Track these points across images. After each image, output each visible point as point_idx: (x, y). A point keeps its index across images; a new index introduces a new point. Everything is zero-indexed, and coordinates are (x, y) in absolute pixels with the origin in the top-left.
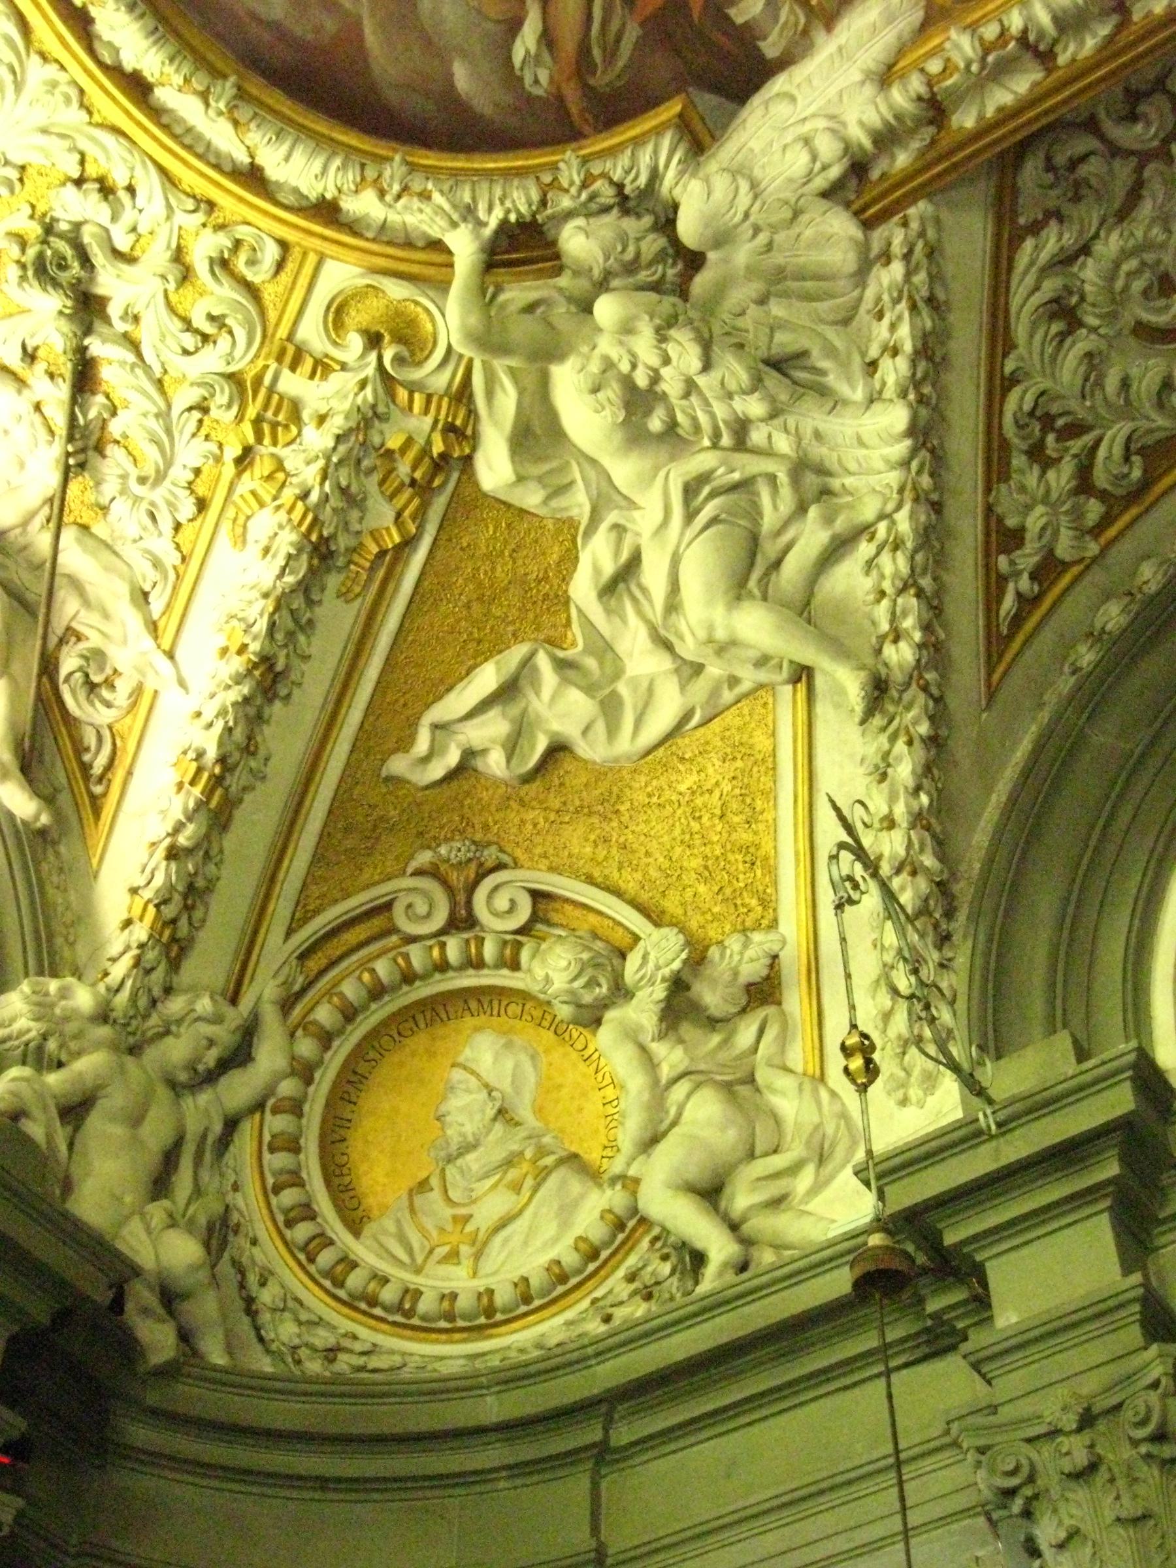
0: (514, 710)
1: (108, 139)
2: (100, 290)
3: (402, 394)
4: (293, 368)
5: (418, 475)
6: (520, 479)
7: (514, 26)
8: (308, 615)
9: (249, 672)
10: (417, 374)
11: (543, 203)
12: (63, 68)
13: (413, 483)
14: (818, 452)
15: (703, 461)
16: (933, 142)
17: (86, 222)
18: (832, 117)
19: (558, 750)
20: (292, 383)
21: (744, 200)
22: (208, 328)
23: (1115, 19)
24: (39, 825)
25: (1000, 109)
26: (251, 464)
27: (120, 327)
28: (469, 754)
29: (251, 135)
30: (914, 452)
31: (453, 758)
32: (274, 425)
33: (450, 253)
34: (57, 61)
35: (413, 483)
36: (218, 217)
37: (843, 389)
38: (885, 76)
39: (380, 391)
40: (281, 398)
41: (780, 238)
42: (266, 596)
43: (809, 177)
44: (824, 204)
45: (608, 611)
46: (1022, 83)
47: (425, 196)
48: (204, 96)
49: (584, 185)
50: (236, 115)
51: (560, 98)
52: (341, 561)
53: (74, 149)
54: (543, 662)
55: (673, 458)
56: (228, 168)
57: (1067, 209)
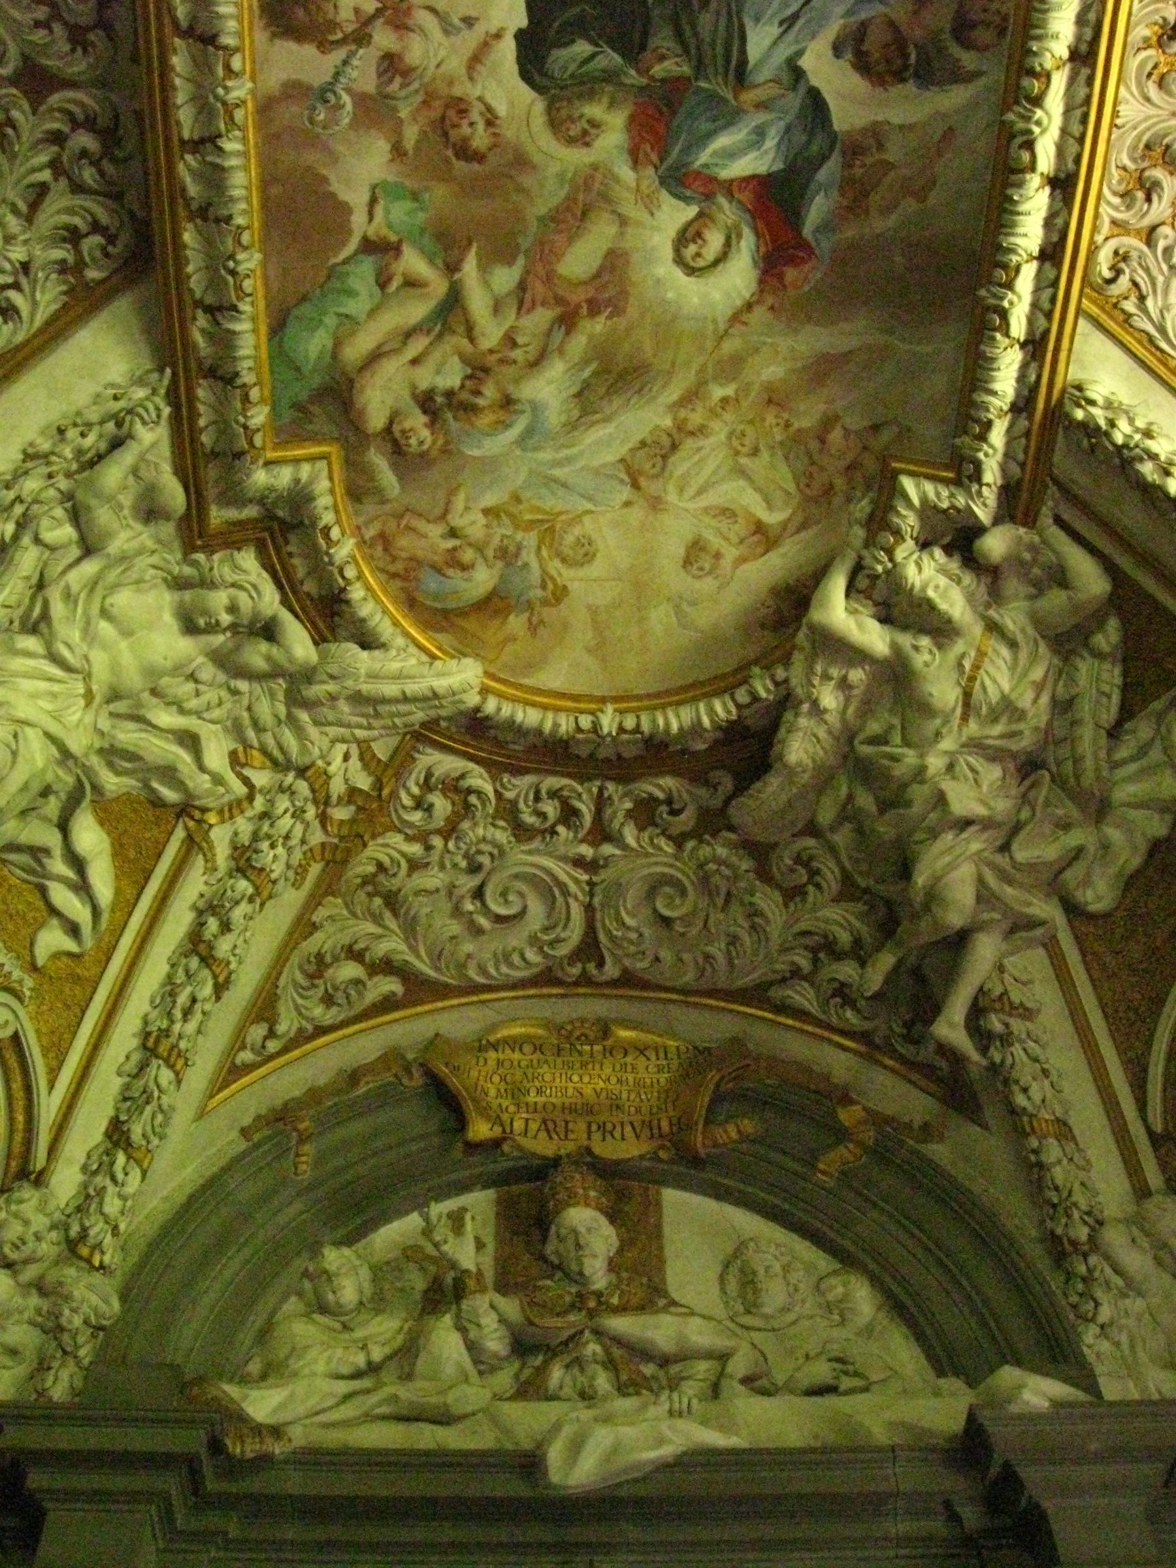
23: (184, 24)
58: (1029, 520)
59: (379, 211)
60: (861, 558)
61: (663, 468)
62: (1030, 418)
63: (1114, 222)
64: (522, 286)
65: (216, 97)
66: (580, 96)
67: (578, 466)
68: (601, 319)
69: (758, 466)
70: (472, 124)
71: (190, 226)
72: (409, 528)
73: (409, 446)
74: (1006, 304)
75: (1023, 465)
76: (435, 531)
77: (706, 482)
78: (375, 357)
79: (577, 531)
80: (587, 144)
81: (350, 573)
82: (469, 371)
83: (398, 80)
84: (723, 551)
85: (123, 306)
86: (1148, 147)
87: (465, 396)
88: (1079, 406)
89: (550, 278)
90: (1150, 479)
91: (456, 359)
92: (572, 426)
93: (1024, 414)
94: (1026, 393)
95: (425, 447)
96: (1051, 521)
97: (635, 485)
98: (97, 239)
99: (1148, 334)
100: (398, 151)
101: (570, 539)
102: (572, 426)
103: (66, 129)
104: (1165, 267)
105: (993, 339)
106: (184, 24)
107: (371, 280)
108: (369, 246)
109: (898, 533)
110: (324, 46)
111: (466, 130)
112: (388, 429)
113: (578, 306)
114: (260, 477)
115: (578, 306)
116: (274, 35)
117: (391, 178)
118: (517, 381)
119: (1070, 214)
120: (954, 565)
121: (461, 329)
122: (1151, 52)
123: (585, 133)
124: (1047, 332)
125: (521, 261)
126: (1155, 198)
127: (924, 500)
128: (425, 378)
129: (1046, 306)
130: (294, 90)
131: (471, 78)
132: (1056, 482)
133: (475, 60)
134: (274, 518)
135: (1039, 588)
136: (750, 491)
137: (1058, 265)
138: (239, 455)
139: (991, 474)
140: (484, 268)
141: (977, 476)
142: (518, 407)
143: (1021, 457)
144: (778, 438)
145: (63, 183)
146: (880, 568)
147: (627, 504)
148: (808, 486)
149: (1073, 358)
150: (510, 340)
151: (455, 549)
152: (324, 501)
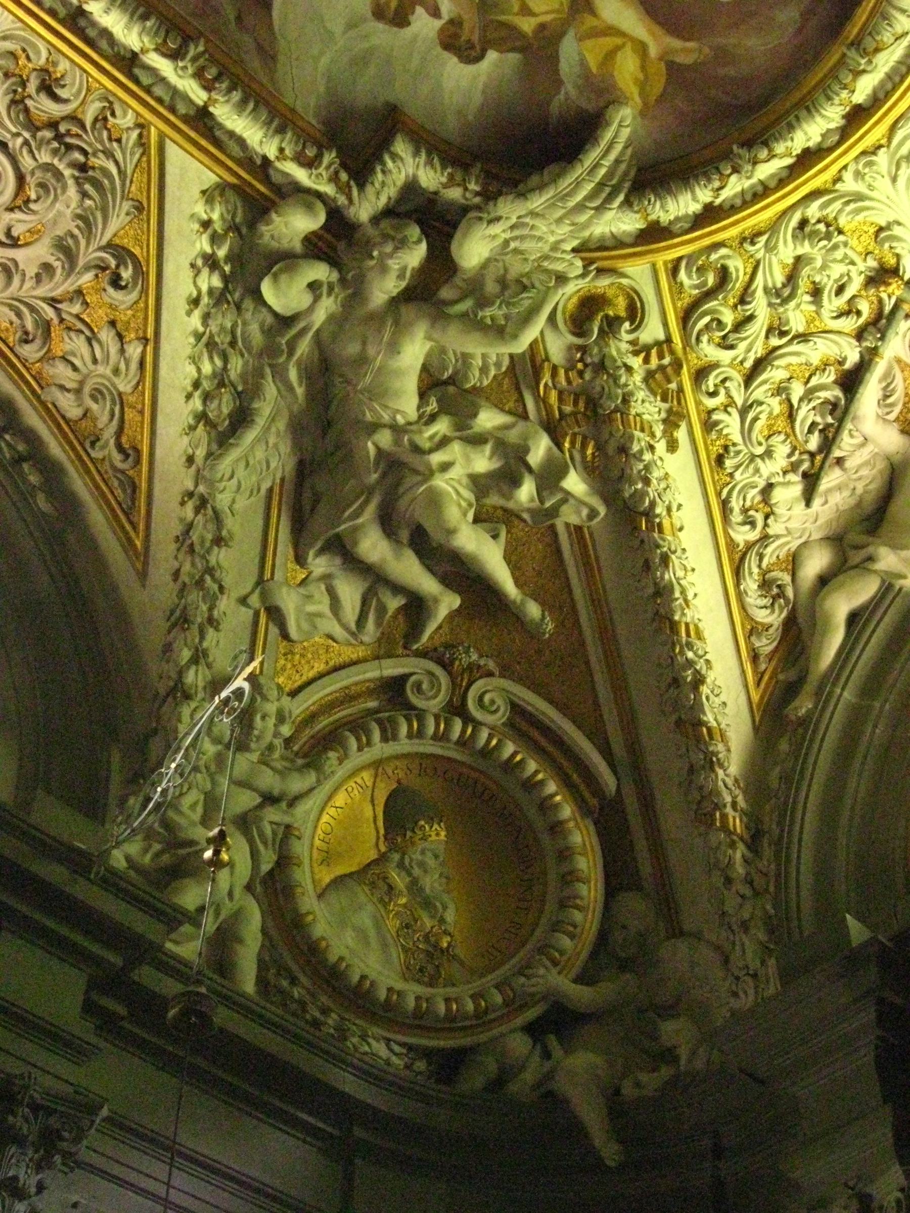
1: (899, 135)
12: (845, 167)
29: (885, 39)
34: (840, 171)
48: (858, 73)
50: (871, 50)
122: (42, 61)
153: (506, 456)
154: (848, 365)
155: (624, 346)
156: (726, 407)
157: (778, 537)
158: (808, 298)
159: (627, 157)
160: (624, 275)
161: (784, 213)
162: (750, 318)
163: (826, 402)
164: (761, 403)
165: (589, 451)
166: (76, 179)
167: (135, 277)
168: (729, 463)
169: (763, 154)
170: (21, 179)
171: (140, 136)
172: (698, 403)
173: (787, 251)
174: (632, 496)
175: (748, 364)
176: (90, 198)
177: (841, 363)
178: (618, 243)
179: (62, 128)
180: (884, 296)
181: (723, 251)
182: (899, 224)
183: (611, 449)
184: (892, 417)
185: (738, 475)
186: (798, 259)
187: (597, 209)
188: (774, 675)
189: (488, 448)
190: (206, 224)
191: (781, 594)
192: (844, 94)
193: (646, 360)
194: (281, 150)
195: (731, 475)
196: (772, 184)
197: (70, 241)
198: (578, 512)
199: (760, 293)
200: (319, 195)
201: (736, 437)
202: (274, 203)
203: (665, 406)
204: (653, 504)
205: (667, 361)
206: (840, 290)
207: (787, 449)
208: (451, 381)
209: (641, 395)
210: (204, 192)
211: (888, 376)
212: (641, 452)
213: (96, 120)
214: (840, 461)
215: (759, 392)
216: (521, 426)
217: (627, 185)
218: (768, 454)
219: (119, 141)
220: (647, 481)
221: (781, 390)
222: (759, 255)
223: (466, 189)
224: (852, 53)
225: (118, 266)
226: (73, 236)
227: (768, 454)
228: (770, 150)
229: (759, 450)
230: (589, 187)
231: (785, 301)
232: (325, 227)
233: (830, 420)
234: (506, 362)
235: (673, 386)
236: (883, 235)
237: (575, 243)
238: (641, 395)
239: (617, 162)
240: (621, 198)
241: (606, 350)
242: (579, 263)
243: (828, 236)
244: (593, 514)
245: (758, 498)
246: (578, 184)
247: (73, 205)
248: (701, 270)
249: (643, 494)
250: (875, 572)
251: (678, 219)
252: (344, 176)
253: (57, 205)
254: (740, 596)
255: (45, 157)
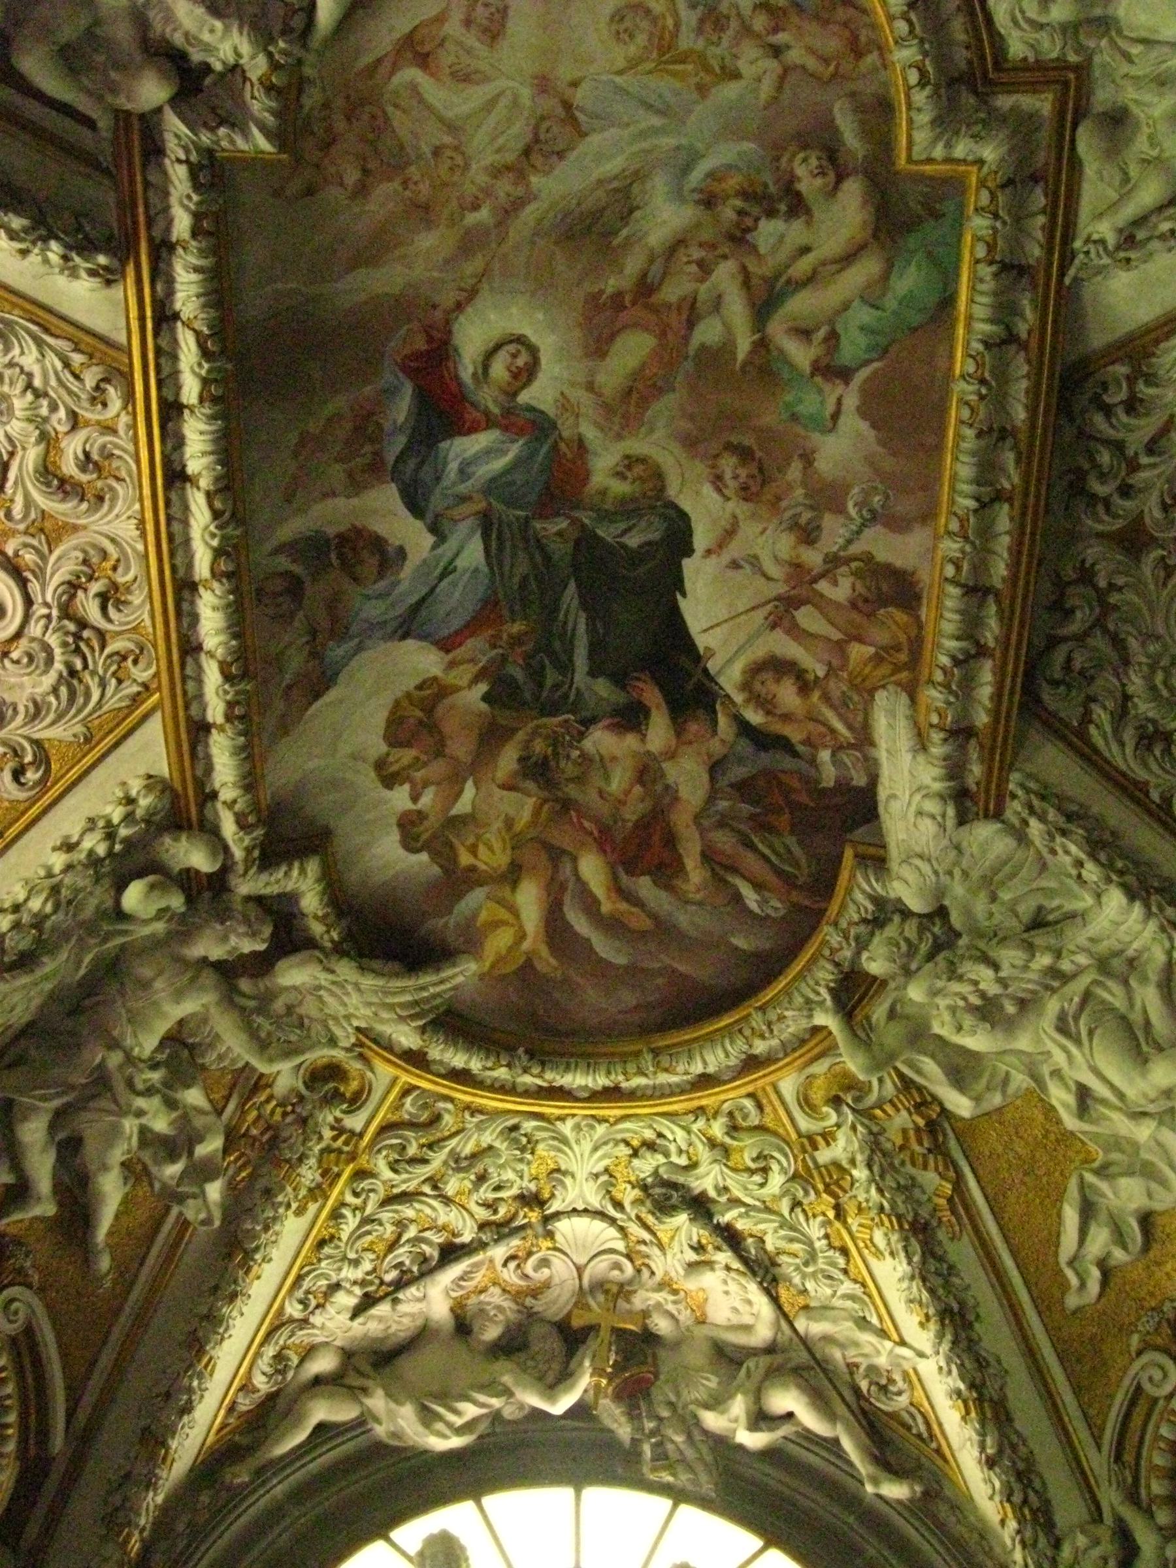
0: (1103, 1216)
2: (697, 1192)
3: (878, 1112)
4: (816, 1148)
5: (926, 1145)
6: (977, 1099)
7: (737, 898)
8: (945, 1266)
9: (943, 1325)
10: (873, 1097)
11: (837, 965)
12: (574, 1115)
13: (930, 1151)
14: (1103, 947)
15: (1053, 1006)
16: (982, 746)
17: (657, 1168)
18: (919, 789)
19: (1146, 1220)
20: (824, 1155)
21: (926, 868)
22: (762, 1164)
23: (991, 599)
24: (918, 1495)
25: (991, 698)
26: (845, 1211)
27: (723, 1199)
28: (1103, 1264)
30: (1147, 906)
31: (1096, 1273)
32: (837, 1183)
33: (826, 1027)
35: (930, 1151)
36: (710, 1112)
37: (1078, 905)
38: (921, 744)
39: (866, 1121)
40: (825, 1166)
41: (965, 864)
42: (912, 1278)
43: (943, 827)
44: (967, 827)
45: (1092, 1122)
46: (986, 674)
47: (781, 1018)
48: (641, 1073)
49: (847, 938)
51: (794, 905)
52: (934, 1223)
53: (617, 1143)
54: (1090, 1178)
55: (1040, 1015)
56: (688, 1087)
57: (1093, 690)
58: (123, 118)
59: (830, 408)
60: (304, 46)
61: (536, 128)
62: (151, 240)
63: (114, 432)
64: (691, 324)
65: (973, 543)
66: (634, 500)
67: (632, 128)
68: (610, 290)
69: (432, 135)
70: (736, 477)
71: (1019, 424)
72: (826, 61)
73: (819, 158)
74: (206, 366)
75: (147, 184)
76: (795, 55)
77: (489, 112)
78: (847, 259)
79: (632, 50)
80: (627, 457)
81: (902, 27)
82: (748, 237)
83: (803, 520)
84: (464, 31)
85: (1098, 340)
86: (101, 499)
87: (755, 210)
88: (106, 268)
89: (663, 334)
90: (11, 215)
91: (762, 251)
92: (639, 176)
93: (158, 241)
94: (162, 265)
95: (801, 155)
96: (100, 124)
97: (567, 106)
98: (1107, 399)
99: (52, 335)
100: (808, 459)
101: (641, 39)
102: (639, 176)
103: (1117, 500)
104: (52, 393)
105: (210, 327)
106: (991, 599)
107: (844, 342)
108: (844, 374)
109: (269, 88)
110: (868, 558)
111: (743, 473)
112: (840, 179)
113: (634, 303)
114: (990, 153)
115: (634, 303)
116: (913, 573)
117: (816, 437)
118: (698, 225)
119: (162, 452)
120: (196, 56)
121: (755, 281)
123: (629, 467)
124: (156, 334)
125: (691, 353)
126: (81, 456)
127: (246, 135)
128: (796, 232)
129: (163, 361)
130: (898, 525)
131: (735, 517)
132: (106, 172)
133: (730, 533)
134: (976, 93)
135: (92, 37)
136: (438, 105)
137: (161, 400)
138: (1010, 182)
139: (179, 174)
140: (727, 346)
141: (194, 172)
142: (696, 196)
143: (154, 199)
144: (413, 169)
145: (1130, 452)
146: (282, 44)
147: (575, 84)
148: (374, 117)
149: (123, 305)
150: (705, 268)
151: (776, 30)
152: (924, 118)
153: (181, 1130)
154: (458, 1240)
155: (330, 1119)
156: (356, 1208)
157: (314, 1327)
158: (473, 1177)
159: (447, 996)
160: (372, 1070)
161: (509, 1111)
162: (425, 1161)
163: (423, 1254)
164: (381, 1224)
165: (244, 1174)
166: (61, 676)
167: (37, 783)
168: (327, 1250)
169: (536, 1070)
170: (18, 635)
171: (139, 693)
172: (342, 1193)
173: (487, 1138)
174: (248, 1231)
175: (396, 1191)
176: (58, 697)
177: (454, 1235)
178: (387, 1046)
179: (86, 634)
180: (521, 1214)
181: (450, 1106)
182: (573, 1176)
183: (261, 1184)
184: (454, 1294)
185: (323, 1264)
186: (490, 1147)
187: (400, 1017)
188: (233, 1432)
189: (174, 1115)
190: (130, 801)
191: (283, 1372)
192: (621, 1078)
193: (335, 1139)
194: (235, 802)
195: (320, 1260)
196: (520, 1089)
197: (10, 712)
198: (198, 1212)
199: (447, 1150)
200: (226, 849)
201: (344, 1236)
202: (190, 827)
203: (319, 1179)
204: (257, 1249)
205: (346, 1149)
206: (498, 1188)
207: (367, 1266)
208: (192, 1048)
209: (312, 1161)
210: (150, 777)
211: (477, 1266)
212: (281, 1204)
213: (117, 653)
214: (396, 1301)
215: (386, 1216)
216: (211, 1119)
217: (432, 1016)
218: (356, 1263)
219: (120, 681)
220: (266, 1228)
221: (401, 1225)
222: (468, 1126)
223: (328, 932)
224: (649, 1057)
225: (30, 763)
226: (15, 710)
227: (356, 1263)
228: (543, 1071)
229: (352, 1255)
230: (408, 998)
231: (459, 1170)
232: (210, 876)
233: (415, 1269)
234: (240, 1065)
235: (336, 1169)
236: (556, 1175)
237: (363, 1025)
238: (312, 1161)
239: (438, 995)
240: (421, 1023)
241: (317, 1112)
242: (353, 1040)
243: (523, 1150)
244: (207, 1222)
245: (324, 1289)
246: (403, 990)
247: (39, 690)
248: (425, 1106)
249: (256, 1237)
250: (361, 1403)
251: (441, 1062)
252: (256, 853)
253: (25, 678)
254: (258, 1355)
255: (53, 640)
